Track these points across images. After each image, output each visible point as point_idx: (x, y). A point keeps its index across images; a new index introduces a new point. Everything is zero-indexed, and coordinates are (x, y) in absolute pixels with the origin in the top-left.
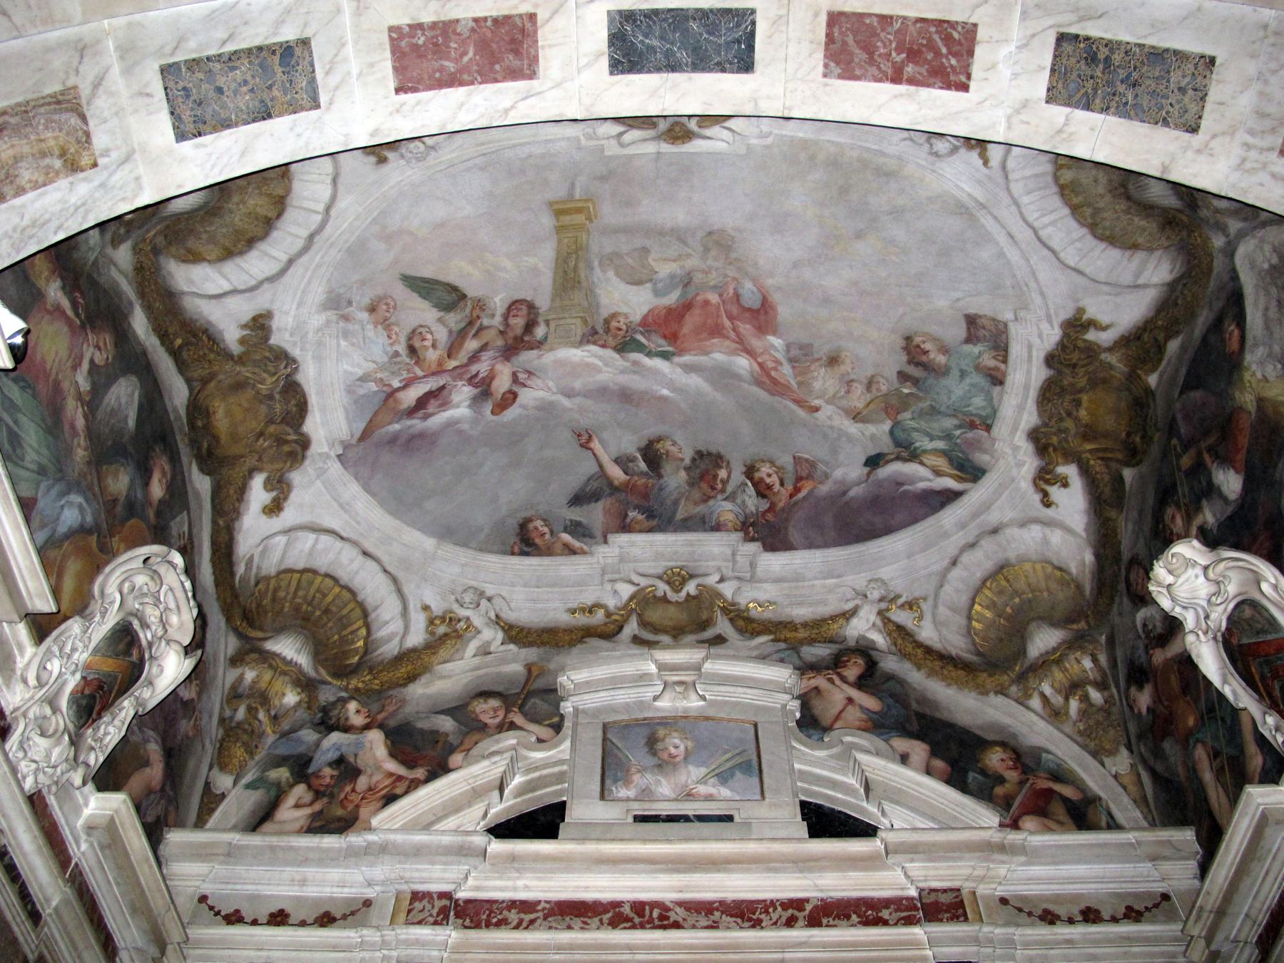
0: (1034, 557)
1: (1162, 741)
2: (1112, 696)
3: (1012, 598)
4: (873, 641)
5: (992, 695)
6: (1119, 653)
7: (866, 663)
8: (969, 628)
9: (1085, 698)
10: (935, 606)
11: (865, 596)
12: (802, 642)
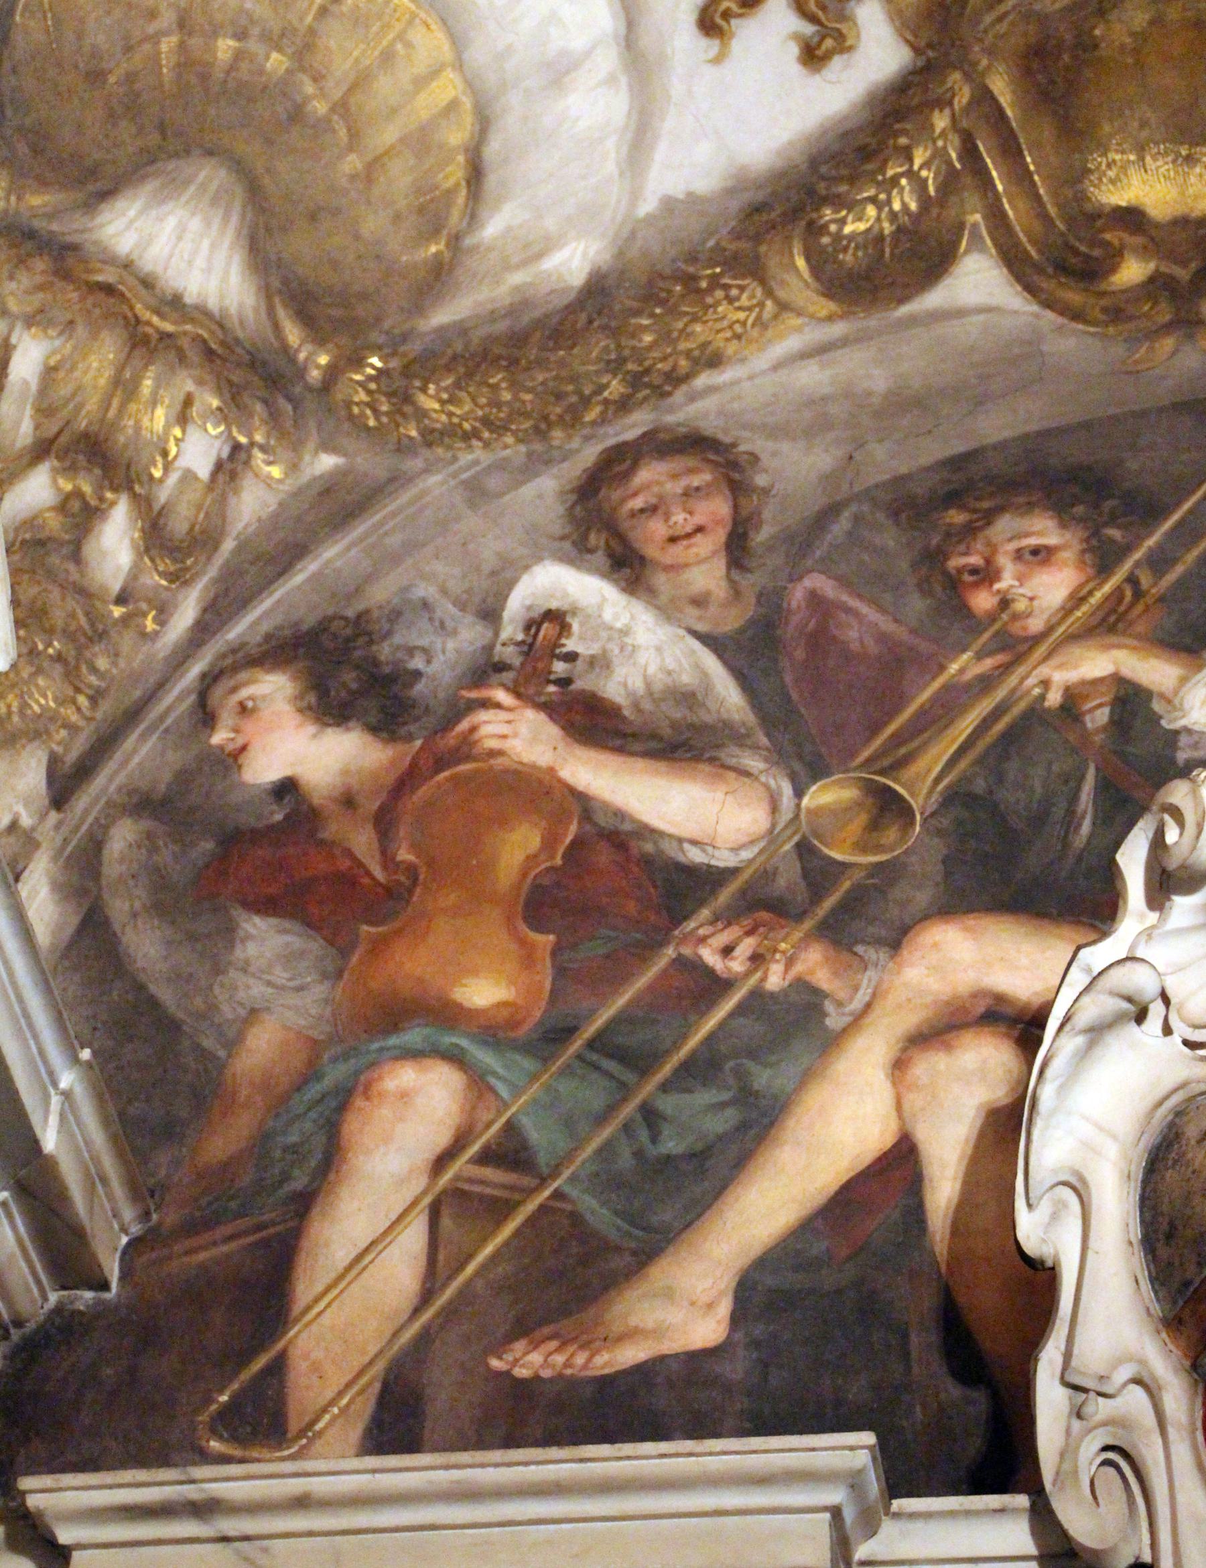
0: (478, 55)
1: (268, 906)
2: (164, 612)
3: (274, 41)
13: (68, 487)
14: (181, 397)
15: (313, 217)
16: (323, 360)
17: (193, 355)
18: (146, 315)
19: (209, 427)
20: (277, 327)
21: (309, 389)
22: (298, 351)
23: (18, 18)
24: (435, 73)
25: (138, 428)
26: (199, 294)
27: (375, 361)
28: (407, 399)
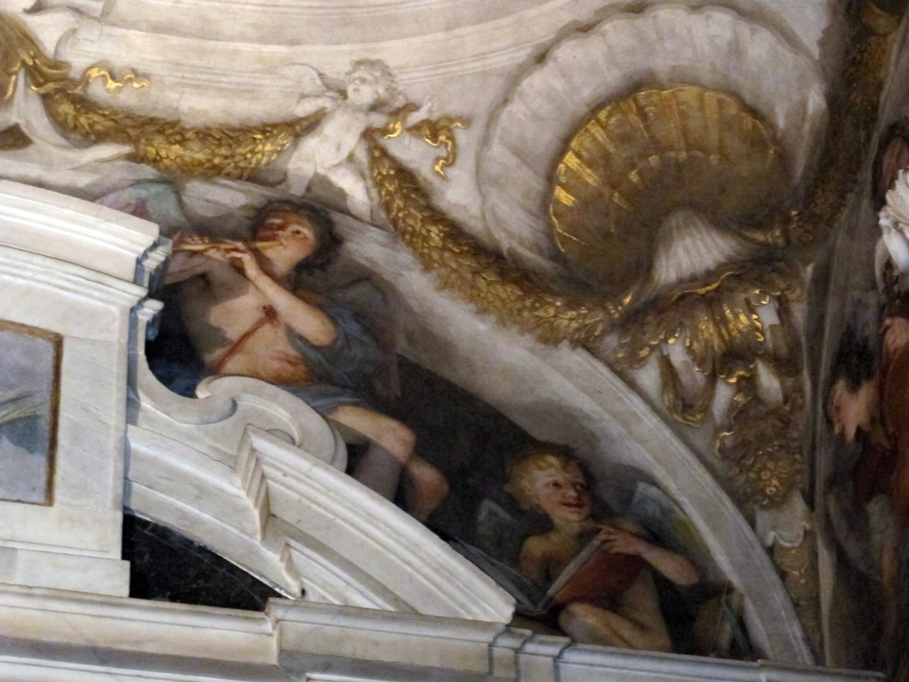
0: (706, 77)
2: (800, 390)
3: (644, 156)
4: (342, 194)
5: (565, 347)
6: (832, 307)
7: (320, 238)
8: (547, 198)
9: (749, 385)
10: (485, 141)
11: (343, 94)
12: (190, 170)
13: (733, 380)
14: (744, 302)
15: (723, 191)
16: (778, 233)
17: (733, 284)
18: (702, 291)
19: (764, 302)
20: (753, 241)
21: (783, 249)
22: (767, 240)
23: (563, 251)
24: (702, 100)
25: (740, 331)
26: (714, 262)
27: (794, 213)
28: (815, 215)
